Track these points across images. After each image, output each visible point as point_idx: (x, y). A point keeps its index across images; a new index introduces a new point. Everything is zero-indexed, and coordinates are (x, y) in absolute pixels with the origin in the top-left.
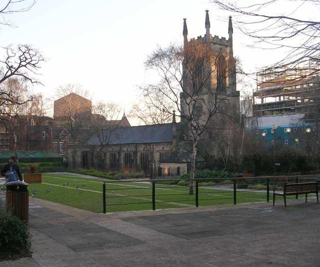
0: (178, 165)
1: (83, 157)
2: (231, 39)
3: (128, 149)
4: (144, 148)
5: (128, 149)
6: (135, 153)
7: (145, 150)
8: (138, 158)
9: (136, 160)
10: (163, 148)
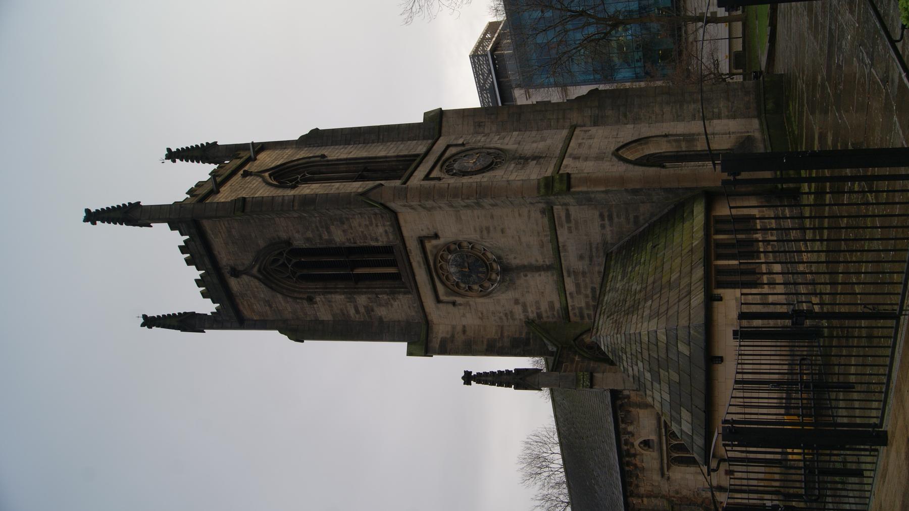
2: (234, 150)
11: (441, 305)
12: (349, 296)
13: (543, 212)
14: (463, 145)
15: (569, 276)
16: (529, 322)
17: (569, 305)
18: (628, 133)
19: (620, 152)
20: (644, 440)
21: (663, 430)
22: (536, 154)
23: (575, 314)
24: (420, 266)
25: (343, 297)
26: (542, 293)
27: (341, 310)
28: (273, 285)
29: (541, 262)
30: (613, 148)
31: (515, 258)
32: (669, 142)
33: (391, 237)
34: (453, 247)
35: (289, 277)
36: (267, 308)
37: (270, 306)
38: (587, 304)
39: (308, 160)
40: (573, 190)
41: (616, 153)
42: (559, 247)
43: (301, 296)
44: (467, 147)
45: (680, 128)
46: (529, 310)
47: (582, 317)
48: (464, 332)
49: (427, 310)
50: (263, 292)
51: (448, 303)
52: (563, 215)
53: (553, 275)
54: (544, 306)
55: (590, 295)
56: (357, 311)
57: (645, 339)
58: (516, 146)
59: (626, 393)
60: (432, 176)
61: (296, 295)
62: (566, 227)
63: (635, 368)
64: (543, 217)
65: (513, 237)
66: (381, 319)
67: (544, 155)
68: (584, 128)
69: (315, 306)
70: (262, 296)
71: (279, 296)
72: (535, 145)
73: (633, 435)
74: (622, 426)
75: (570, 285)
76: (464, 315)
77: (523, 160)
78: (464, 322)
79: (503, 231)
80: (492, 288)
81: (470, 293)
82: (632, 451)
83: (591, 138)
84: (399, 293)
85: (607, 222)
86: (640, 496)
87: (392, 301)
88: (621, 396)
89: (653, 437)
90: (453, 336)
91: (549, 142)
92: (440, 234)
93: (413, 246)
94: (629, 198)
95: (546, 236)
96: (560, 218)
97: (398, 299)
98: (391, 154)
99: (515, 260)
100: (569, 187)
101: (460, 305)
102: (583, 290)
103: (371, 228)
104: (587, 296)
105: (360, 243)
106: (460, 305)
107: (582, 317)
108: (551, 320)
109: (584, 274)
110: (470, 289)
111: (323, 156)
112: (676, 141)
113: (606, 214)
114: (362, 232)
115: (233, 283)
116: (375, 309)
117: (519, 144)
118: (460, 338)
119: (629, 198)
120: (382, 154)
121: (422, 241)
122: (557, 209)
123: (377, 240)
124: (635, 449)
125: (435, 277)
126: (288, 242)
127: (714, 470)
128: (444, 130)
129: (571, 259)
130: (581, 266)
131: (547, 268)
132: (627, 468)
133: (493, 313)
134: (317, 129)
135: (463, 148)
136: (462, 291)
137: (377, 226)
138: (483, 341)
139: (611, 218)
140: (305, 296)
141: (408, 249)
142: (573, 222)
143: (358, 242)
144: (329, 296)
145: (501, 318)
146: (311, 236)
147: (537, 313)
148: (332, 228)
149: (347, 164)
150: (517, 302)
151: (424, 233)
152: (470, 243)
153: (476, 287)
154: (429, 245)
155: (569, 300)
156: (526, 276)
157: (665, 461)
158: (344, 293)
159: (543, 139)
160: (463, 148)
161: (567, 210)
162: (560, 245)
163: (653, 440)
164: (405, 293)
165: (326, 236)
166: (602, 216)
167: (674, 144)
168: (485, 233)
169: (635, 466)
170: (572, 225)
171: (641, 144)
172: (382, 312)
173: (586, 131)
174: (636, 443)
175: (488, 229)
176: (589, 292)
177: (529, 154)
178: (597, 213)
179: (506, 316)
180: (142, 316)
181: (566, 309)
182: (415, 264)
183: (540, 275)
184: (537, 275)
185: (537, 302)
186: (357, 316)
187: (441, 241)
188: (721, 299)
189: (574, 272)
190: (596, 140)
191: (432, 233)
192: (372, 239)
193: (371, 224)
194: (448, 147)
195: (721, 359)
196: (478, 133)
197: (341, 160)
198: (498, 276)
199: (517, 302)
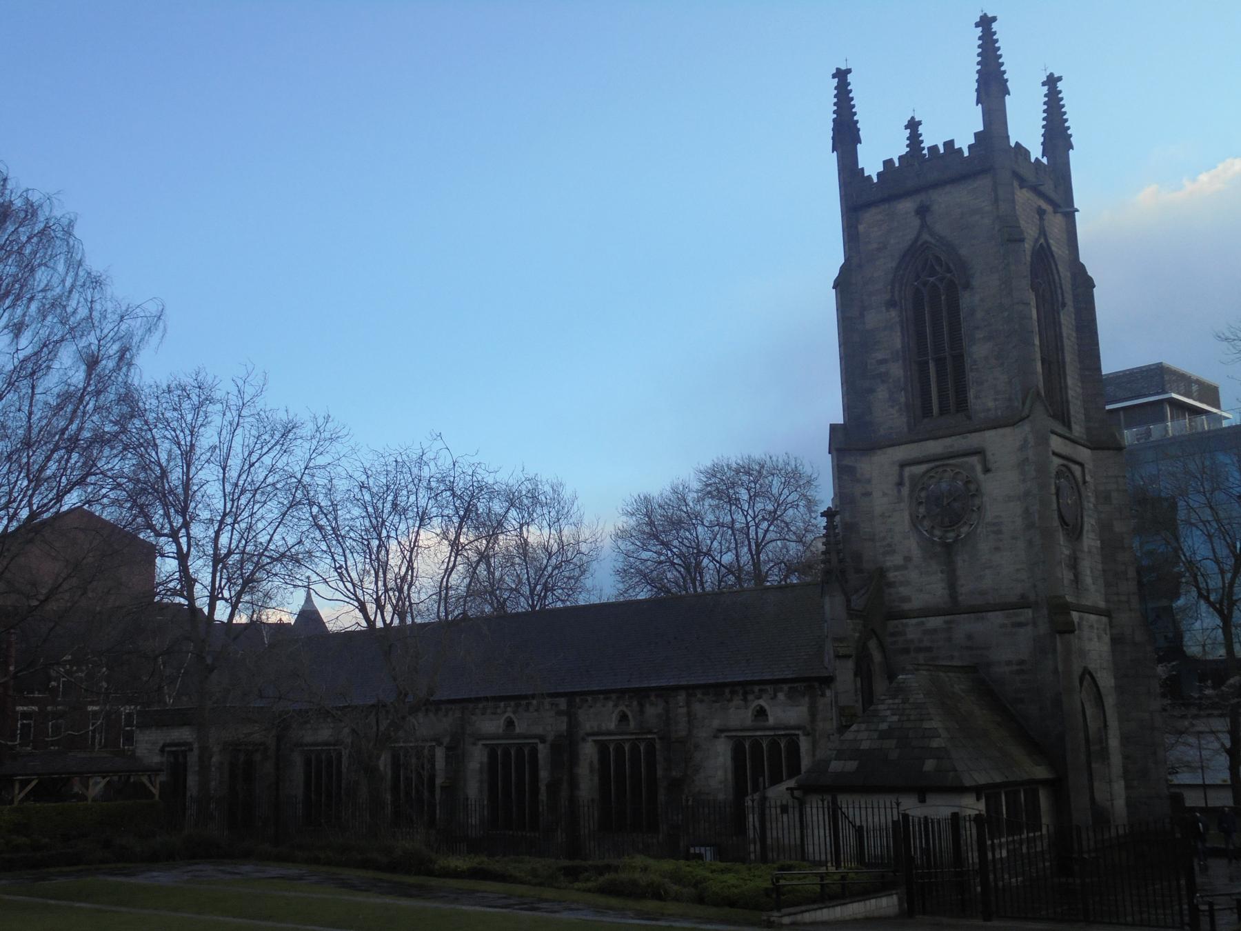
3: (510, 723)
4: (623, 718)
5: (510, 723)
6: (565, 748)
9: (574, 784)
11: (896, 468)
13: (1023, 596)
14: (1085, 482)
16: (882, 572)
17: (908, 620)
18: (1106, 681)
20: (765, 710)
21: (783, 733)
25: (899, 346)
26: (921, 590)
30: (1091, 666)
31: (964, 561)
40: (1057, 636)
42: (981, 612)
44: (1082, 489)
45: (1114, 743)
49: (890, 451)
51: (901, 476)
52: (1022, 619)
54: (904, 591)
57: (926, 725)
59: (828, 693)
62: (1006, 622)
63: (888, 713)
66: (871, 391)
67: (1079, 587)
69: (884, 309)
71: (894, 264)
72: (1088, 572)
73: (772, 699)
74: (786, 687)
75: (935, 622)
76: (885, 494)
79: (997, 549)
80: (922, 530)
83: (1099, 638)
85: (1015, 668)
86: (688, 704)
87: (897, 407)
88: (823, 686)
89: (771, 721)
92: (989, 475)
93: (973, 440)
97: (901, 415)
98: (1071, 393)
100: (1061, 632)
101: (899, 491)
106: (899, 491)
107: (893, 635)
110: (921, 503)
111: (1064, 305)
115: (906, 206)
117: (1090, 552)
120: (1070, 382)
122: (1029, 613)
123: (977, 397)
124: (754, 701)
126: (967, 286)
127: (792, 794)
129: (966, 626)
132: (727, 691)
134: (1094, 286)
135: (1081, 484)
137: (995, 400)
141: (968, 435)
147: (894, 582)
150: (908, 559)
151: (989, 454)
152: (979, 508)
153: (922, 510)
154: (974, 460)
155: (914, 621)
156: (942, 572)
160: (1081, 484)
162: (984, 614)
163: (767, 720)
165: (979, 335)
166: (1022, 662)
169: (731, 700)
172: (882, 393)
173: (1105, 630)
174: (762, 702)
175: (999, 532)
179: (888, 544)
180: (848, 68)
181: (904, 615)
183: (944, 589)
187: (981, 476)
188: (978, 799)
194: (1081, 465)
195: (922, 800)
197: (1060, 328)
198: (939, 539)
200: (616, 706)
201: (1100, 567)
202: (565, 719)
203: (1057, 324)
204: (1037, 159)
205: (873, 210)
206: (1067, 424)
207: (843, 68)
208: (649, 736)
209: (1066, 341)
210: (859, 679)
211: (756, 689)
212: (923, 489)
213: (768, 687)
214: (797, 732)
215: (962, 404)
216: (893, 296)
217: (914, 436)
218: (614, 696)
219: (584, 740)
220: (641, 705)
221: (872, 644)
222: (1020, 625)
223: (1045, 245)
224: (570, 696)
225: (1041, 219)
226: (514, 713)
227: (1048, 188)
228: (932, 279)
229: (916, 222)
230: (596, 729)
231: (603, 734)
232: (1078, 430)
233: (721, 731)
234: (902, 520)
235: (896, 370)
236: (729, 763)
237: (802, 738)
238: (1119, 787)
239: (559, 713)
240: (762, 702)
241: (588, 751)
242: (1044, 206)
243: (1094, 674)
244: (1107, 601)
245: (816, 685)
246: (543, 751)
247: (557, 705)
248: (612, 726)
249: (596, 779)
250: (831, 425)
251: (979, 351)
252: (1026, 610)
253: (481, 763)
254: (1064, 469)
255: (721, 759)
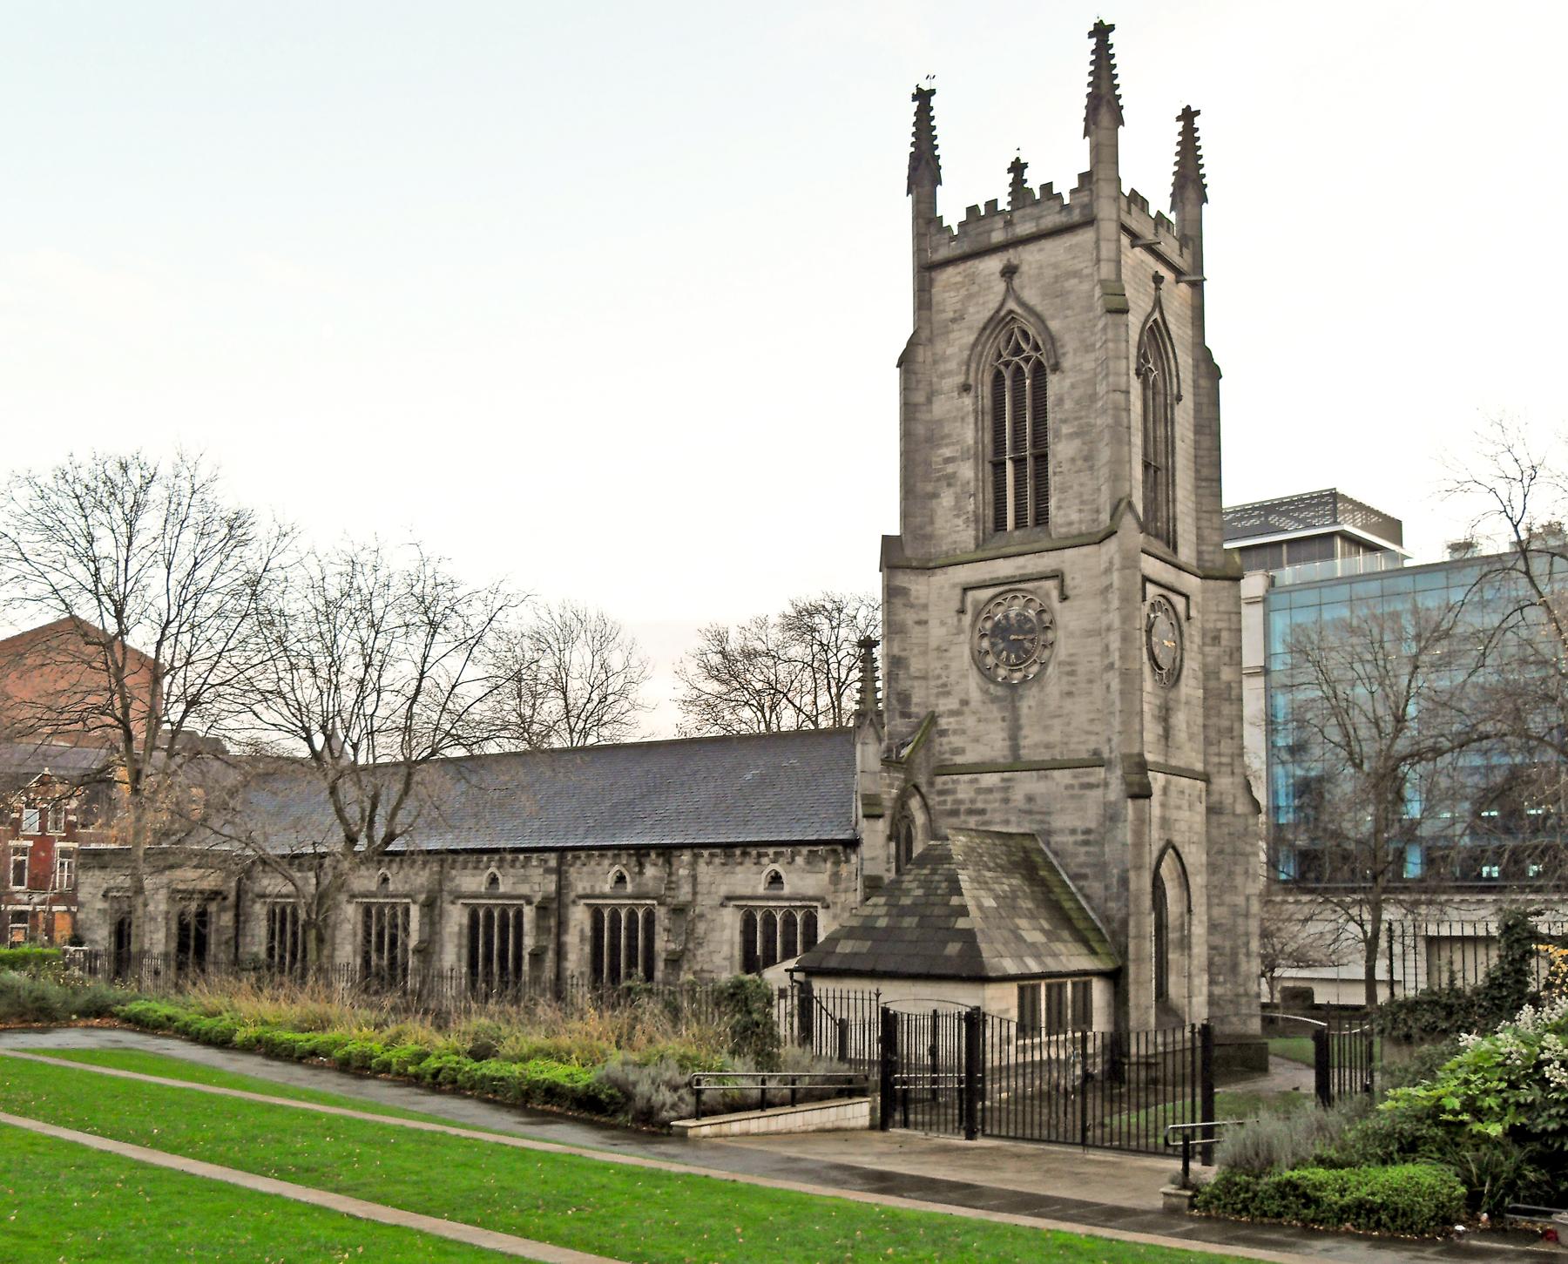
0: (964, 997)
1: (183, 928)
2: (1192, 239)
3: (494, 880)
4: (621, 879)
5: (494, 880)
6: (553, 910)
7: (629, 888)
8: (572, 939)
10: (776, 879)
11: (958, 591)
12: (972, 452)
13: (1096, 753)
14: (1188, 618)
15: (1003, 780)
16: (933, 718)
18: (1195, 857)
19: (1170, 851)
21: (799, 904)
22: (1171, 732)
23: (945, 783)
24: (1019, 568)
25: (971, 442)
27: (949, 436)
28: (988, 332)
29: (1023, 743)
30: (1177, 839)
31: (1030, 707)
32: (1182, 915)
33: (1063, 530)
34: (1046, 617)
35: (1000, 356)
36: (951, 315)
37: (954, 320)
38: (961, 802)
39: (1174, 373)
41: (1170, 845)
43: (972, 374)
45: (1199, 930)
46: (952, 720)
47: (941, 793)
48: (919, 623)
50: (979, 314)
51: (963, 601)
52: (1092, 780)
53: (1004, 757)
54: (957, 741)
55: (974, 807)
56: (948, 460)
58: (1183, 699)
59: (853, 858)
60: (1149, 586)
61: (973, 366)
64: (1088, 751)
65: (1060, 707)
66: (935, 495)
68: (1204, 794)
69: (955, 394)
70: (971, 310)
71: (972, 338)
72: (1184, 726)
73: (789, 863)
74: (805, 850)
76: (943, 623)
77: (1165, 715)
78: (933, 623)
79: (1070, 694)
81: (977, 635)
82: (765, 860)
83: (1191, 807)
84: (977, 530)
85: (1080, 837)
86: (693, 864)
90: (912, 606)
91: (1187, 747)
92: (1067, 603)
93: (1048, 562)
94: (1115, 871)
95: (1062, 753)
96: (1088, 774)
99: (1028, 704)
100: (1134, 797)
101: (960, 620)
102: (981, 797)
103: (1077, 501)
104: (973, 801)
105: (1054, 481)
106: (960, 620)
107: (941, 793)
108: (937, 748)
109: (1006, 801)
110: (984, 636)
111: (1179, 398)
112: (1182, 925)
113: (1091, 837)
114: (1071, 487)
115: (992, 265)
116: (952, 490)
117: (1187, 703)
118: (909, 617)
119: (1115, 871)
121: (1057, 575)
122: (1100, 773)
125: (1002, 589)
126: (1056, 368)
127: (792, 977)
128: (1211, 583)
129: (1027, 784)
130: (1018, 796)
131: (1015, 748)
133: (946, 667)
136: (979, 625)
137: (1080, 511)
138: (905, 650)
139: (1086, 843)
140: (971, 381)
142: (1082, 792)
143: (1057, 478)
144: (971, 419)
145: (939, 677)
146: (1066, 407)
147: (947, 730)
148: (1077, 442)
149: (1166, 437)
150: (965, 703)
151: (1068, 581)
153: (985, 644)
154: (1050, 585)
155: (967, 777)
156: (1003, 719)
157: (751, 903)
158: (976, 443)
159: (1191, 737)
161: (1098, 786)
164: (976, 538)
165: (1065, 429)
166: (1088, 832)
167: (1178, 923)
168: (1068, 668)
170: (1077, 791)
171: (1179, 877)
172: (947, 499)
174: (776, 867)
175: (1072, 673)
176: (980, 805)
177: (1173, 721)
178: (1093, 825)
182: (1021, 560)
183: (1004, 740)
184: (1004, 735)
185: (964, 732)
186: (940, 459)
189: (1008, 788)
190: (1188, 813)
191: (1069, 592)
192: (1060, 500)
193: (1082, 503)
194: (1187, 597)
196: (1204, 636)
199: (965, 703)
200: (612, 865)
201: (1200, 721)
202: (554, 877)
203: (1169, 422)
204: (1159, 213)
205: (950, 270)
206: (1172, 544)
207: (926, 87)
208: (648, 902)
209: (1178, 443)
210: (893, 845)
211: (771, 851)
212: (988, 618)
213: (783, 849)
214: (814, 904)
215: (1042, 517)
216: (967, 378)
217: (983, 551)
218: (610, 853)
219: (574, 902)
220: (641, 865)
221: (915, 803)
222: (1089, 786)
223: (1160, 320)
224: (562, 851)
225: (1158, 289)
226: (499, 868)
227: (1169, 247)
228: (1016, 359)
229: (1000, 286)
230: (588, 891)
231: (598, 897)
232: (1186, 554)
233: (729, 898)
234: (962, 653)
235: (967, 471)
236: (737, 938)
237: (820, 911)
238: (1201, 981)
239: (548, 871)
240: (776, 867)
241: (579, 917)
242: (1163, 271)
243: (1180, 850)
244: (1206, 763)
245: (840, 848)
246: (529, 913)
247: (546, 861)
248: (607, 889)
249: (587, 949)
250: (884, 537)
251: (1061, 451)
252: (1097, 769)
253: (461, 925)
254: (1162, 600)
255: (727, 934)
